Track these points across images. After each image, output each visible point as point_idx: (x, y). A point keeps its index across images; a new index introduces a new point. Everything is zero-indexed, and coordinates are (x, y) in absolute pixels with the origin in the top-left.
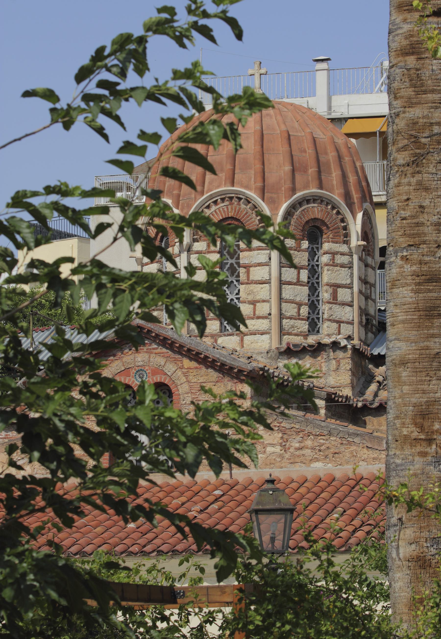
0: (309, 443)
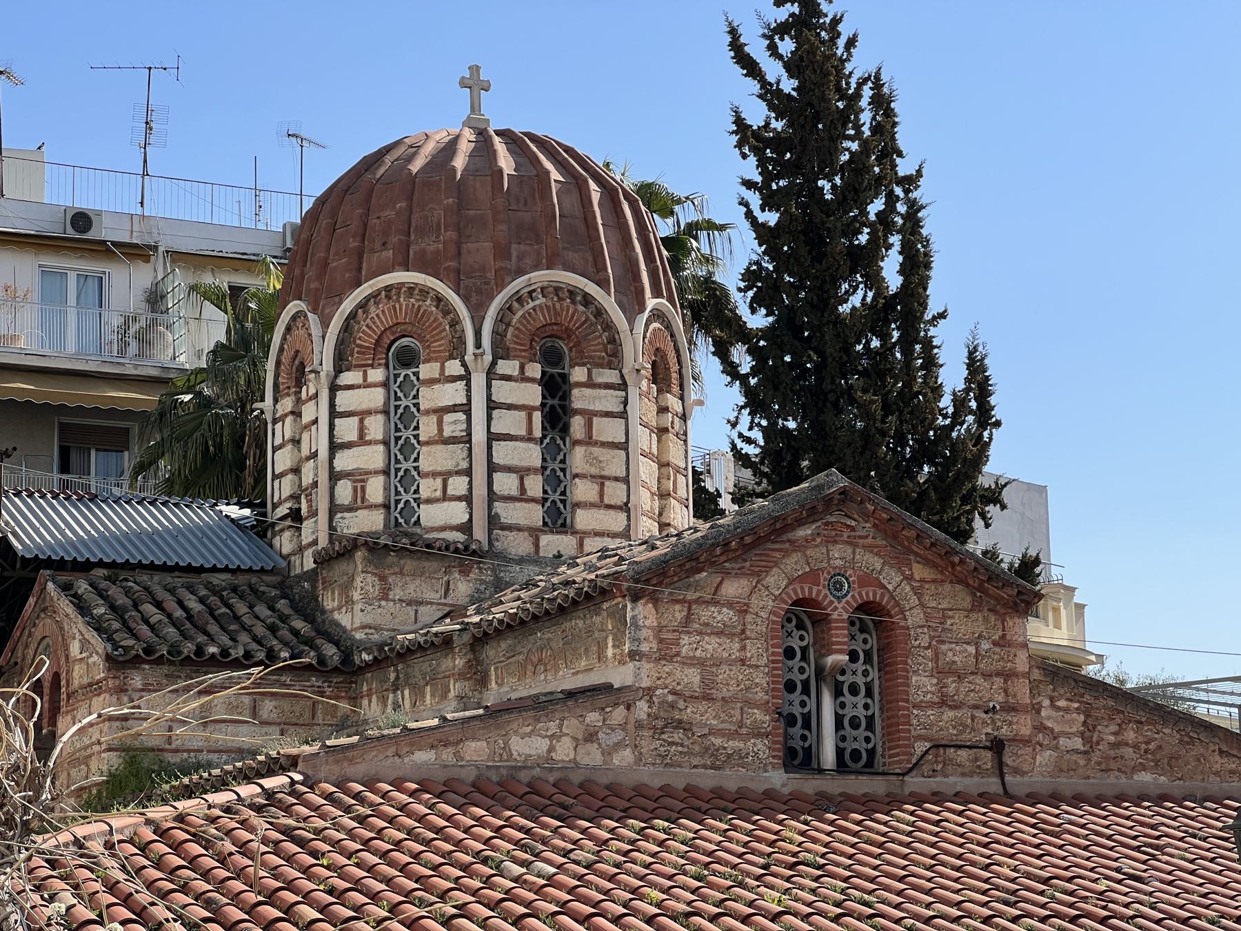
0: (1130, 735)
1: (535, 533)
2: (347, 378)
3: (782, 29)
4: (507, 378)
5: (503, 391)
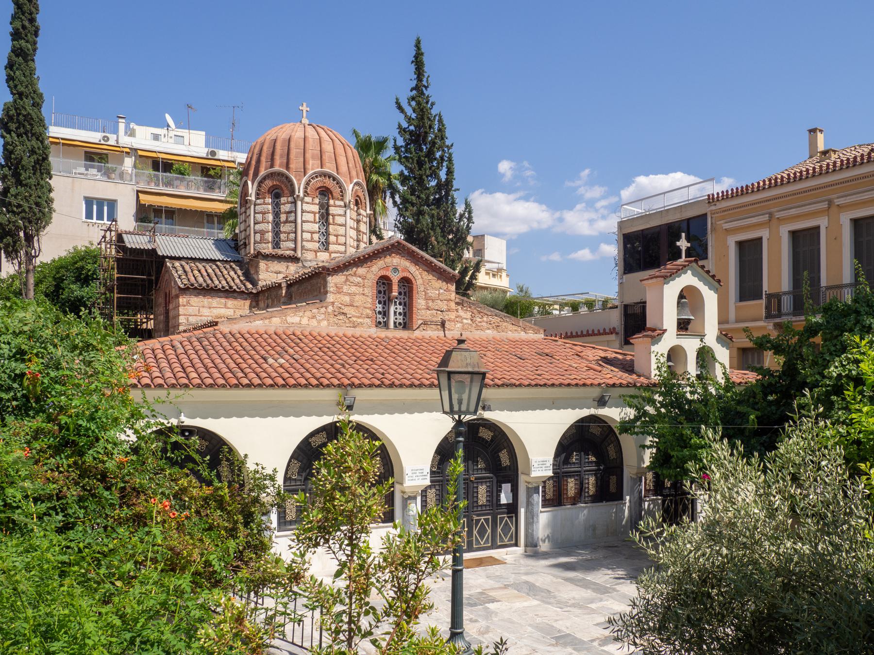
0: (485, 319)
1: (316, 252)
2: (258, 201)
3: (413, 99)
4: (307, 203)
5: (306, 207)
